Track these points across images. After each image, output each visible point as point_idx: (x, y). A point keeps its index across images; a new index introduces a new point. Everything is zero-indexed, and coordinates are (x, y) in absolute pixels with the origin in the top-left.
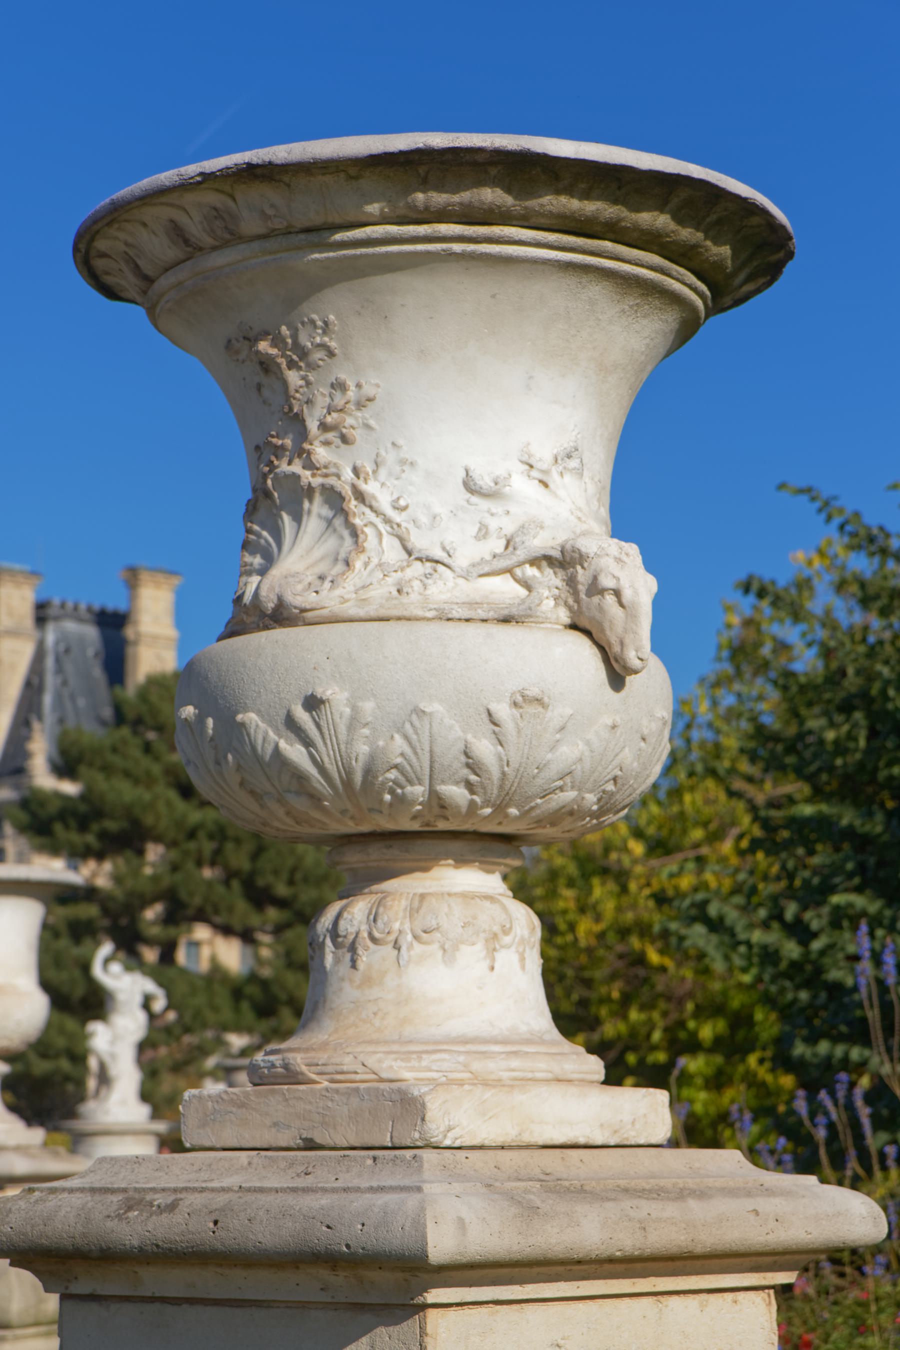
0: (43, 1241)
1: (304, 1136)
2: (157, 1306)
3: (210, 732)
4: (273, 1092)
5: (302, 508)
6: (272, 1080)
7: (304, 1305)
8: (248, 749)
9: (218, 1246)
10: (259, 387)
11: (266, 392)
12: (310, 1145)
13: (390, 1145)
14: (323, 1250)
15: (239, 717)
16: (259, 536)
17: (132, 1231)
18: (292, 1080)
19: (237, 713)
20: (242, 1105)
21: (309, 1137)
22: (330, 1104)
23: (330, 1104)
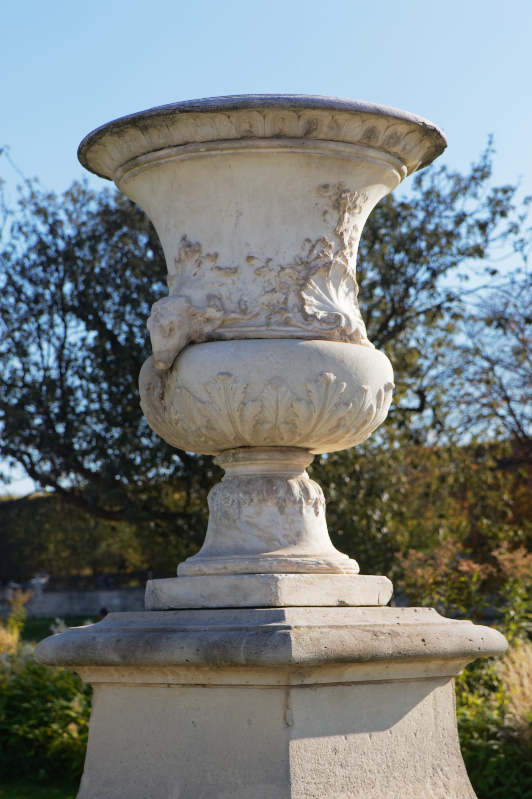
0: (344, 654)
1: (340, 600)
2: (339, 687)
3: (343, 390)
4: (326, 577)
5: (340, 283)
6: (318, 571)
7: (406, 681)
8: (361, 403)
9: (428, 652)
10: (325, 213)
11: (328, 217)
12: (342, 605)
13: (377, 604)
14: (469, 650)
15: (364, 386)
16: (315, 288)
17: (387, 647)
18: (331, 571)
19: (363, 384)
20: (311, 584)
21: (343, 600)
22: (352, 584)
23: (352, 584)
